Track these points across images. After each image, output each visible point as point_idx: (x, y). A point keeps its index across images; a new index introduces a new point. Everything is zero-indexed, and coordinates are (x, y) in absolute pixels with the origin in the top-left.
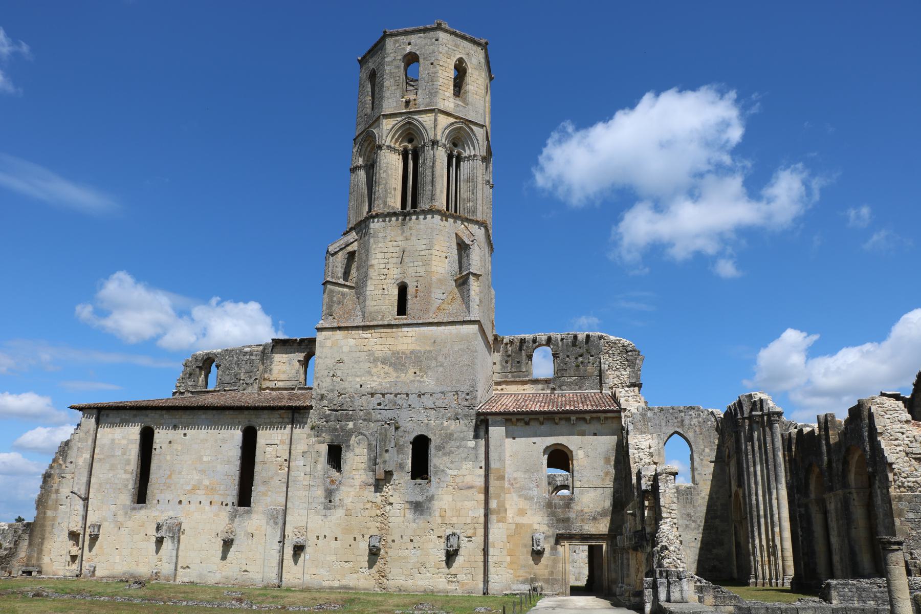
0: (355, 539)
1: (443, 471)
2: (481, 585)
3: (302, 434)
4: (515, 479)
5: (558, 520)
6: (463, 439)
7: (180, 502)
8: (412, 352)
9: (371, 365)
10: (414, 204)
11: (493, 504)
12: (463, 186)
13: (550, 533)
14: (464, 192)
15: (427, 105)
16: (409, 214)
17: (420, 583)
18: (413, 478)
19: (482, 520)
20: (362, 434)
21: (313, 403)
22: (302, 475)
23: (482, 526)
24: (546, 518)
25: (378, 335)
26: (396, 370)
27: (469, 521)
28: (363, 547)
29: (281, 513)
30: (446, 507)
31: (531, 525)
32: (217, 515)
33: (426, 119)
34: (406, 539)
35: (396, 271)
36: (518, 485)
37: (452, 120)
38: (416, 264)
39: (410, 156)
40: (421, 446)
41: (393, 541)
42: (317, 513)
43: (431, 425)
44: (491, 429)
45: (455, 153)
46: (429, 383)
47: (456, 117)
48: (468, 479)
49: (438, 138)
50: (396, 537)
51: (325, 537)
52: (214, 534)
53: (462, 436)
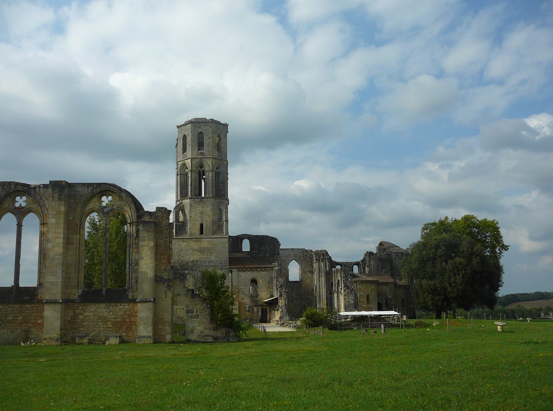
46: (213, 258)
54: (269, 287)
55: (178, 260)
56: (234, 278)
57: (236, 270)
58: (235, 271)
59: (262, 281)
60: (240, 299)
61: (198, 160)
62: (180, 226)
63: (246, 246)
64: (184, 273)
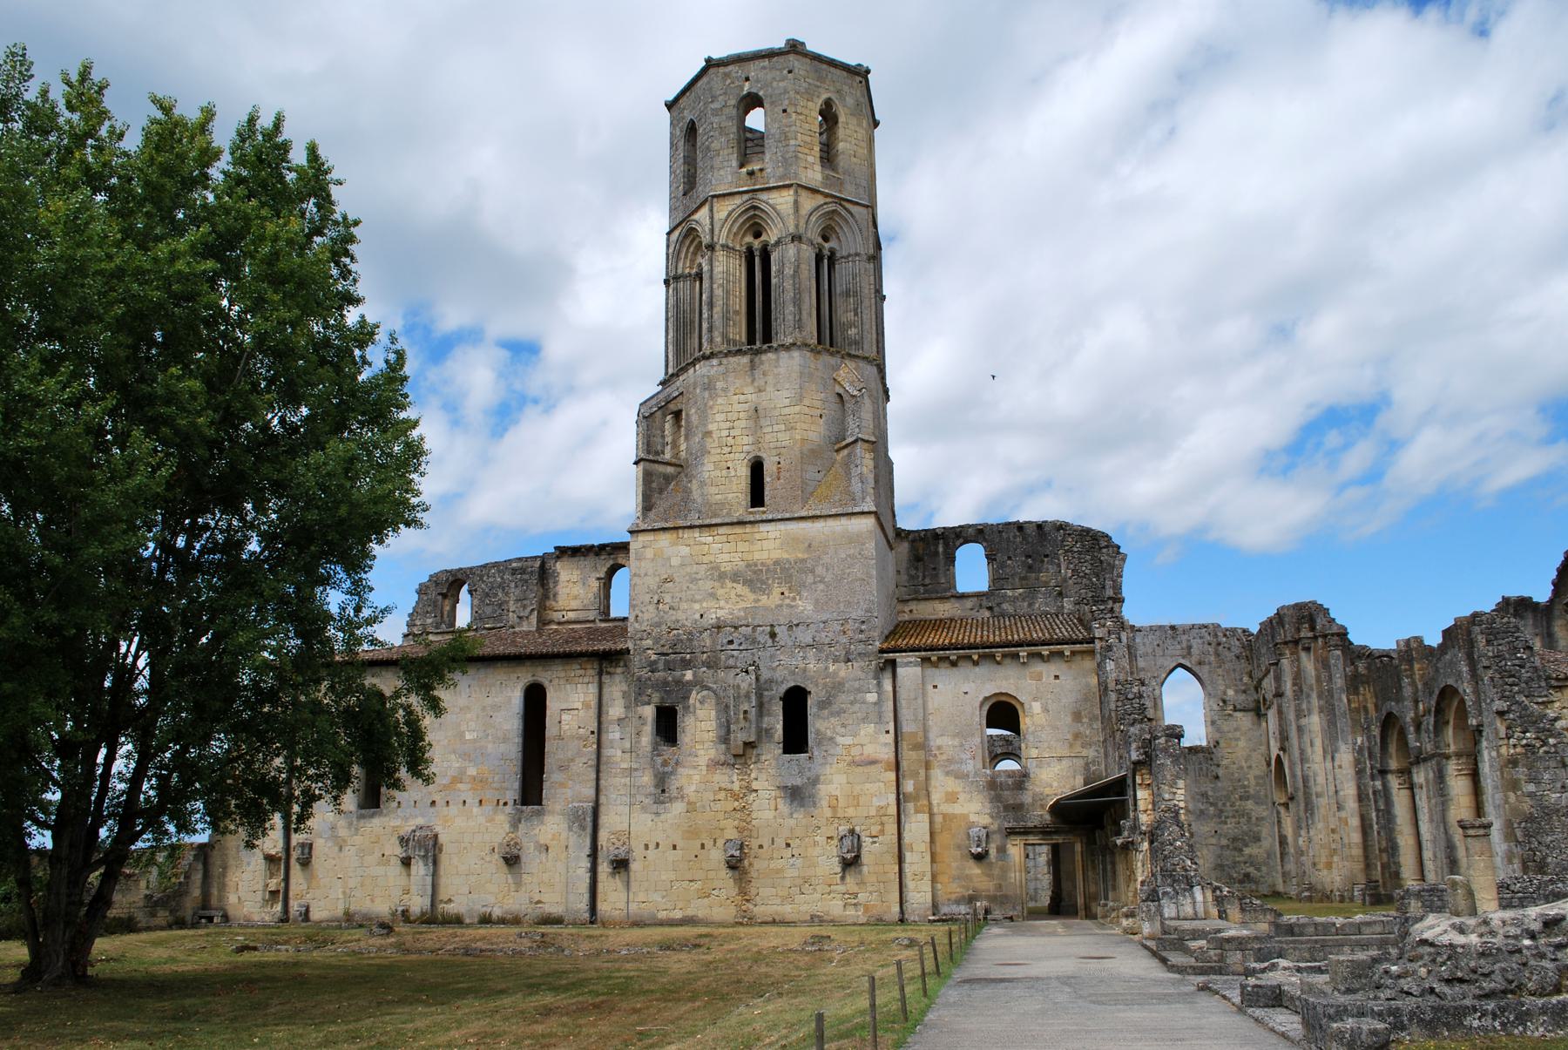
0: (703, 846)
1: (831, 739)
2: (897, 909)
3: (617, 688)
4: (939, 748)
5: (1007, 808)
6: (859, 690)
7: (433, 803)
8: (777, 563)
9: (717, 584)
10: (767, 338)
11: (909, 786)
12: (839, 302)
13: (994, 827)
14: (844, 314)
15: (781, 178)
16: (758, 352)
17: (804, 908)
18: (786, 751)
19: (893, 810)
20: (709, 689)
21: (630, 645)
22: (619, 753)
23: (894, 819)
24: (988, 805)
25: (724, 538)
26: (753, 591)
27: (873, 812)
28: (717, 856)
29: (590, 812)
30: (837, 793)
31: (965, 817)
32: (491, 820)
33: (781, 200)
34: (780, 842)
35: (746, 440)
36: (944, 757)
37: (820, 200)
38: (776, 428)
39: (757, 260)
40: (796, 701)
41: (761, 847)
42: (644, 809)
43: (811, 670)
44: (900, 670)
45: (826, 253)
46: (805, 606)
47: (827, 195)
48: (870, 751)
49: (802, 230)
50: (766, 843)
51: (658, 845)
52: (487, 850)
53: (856, 685)
54: (1077, 736)
55: (658, 625)
56: (903, 694)
57: (912, 657)
58: (909, 671)
59: (1046, 710)
60: (936, 798)
61: (738, 200)
62: (668, 479)
63: (972, 570)
64: (679, 682)
